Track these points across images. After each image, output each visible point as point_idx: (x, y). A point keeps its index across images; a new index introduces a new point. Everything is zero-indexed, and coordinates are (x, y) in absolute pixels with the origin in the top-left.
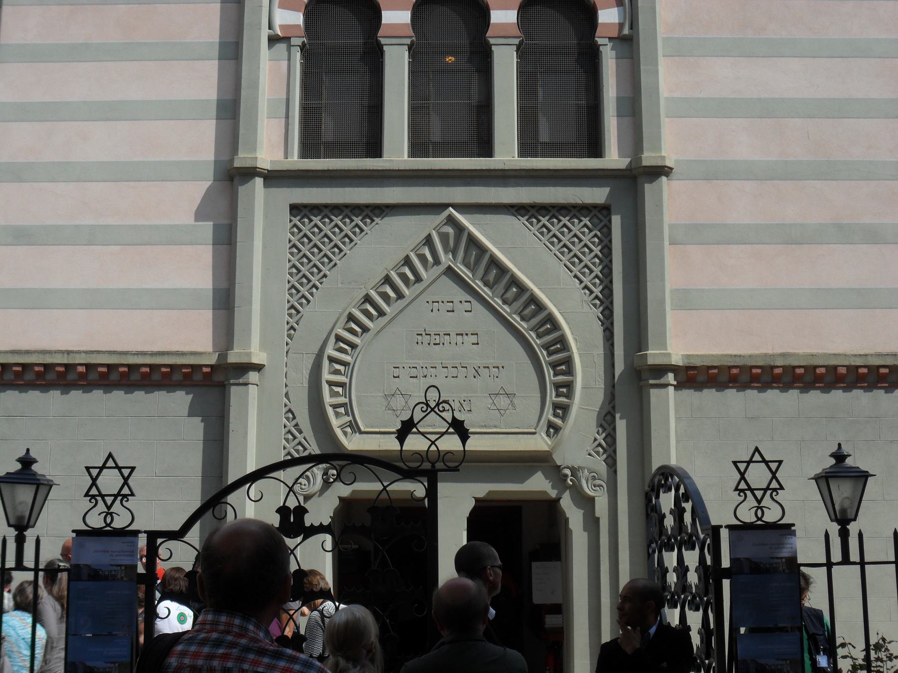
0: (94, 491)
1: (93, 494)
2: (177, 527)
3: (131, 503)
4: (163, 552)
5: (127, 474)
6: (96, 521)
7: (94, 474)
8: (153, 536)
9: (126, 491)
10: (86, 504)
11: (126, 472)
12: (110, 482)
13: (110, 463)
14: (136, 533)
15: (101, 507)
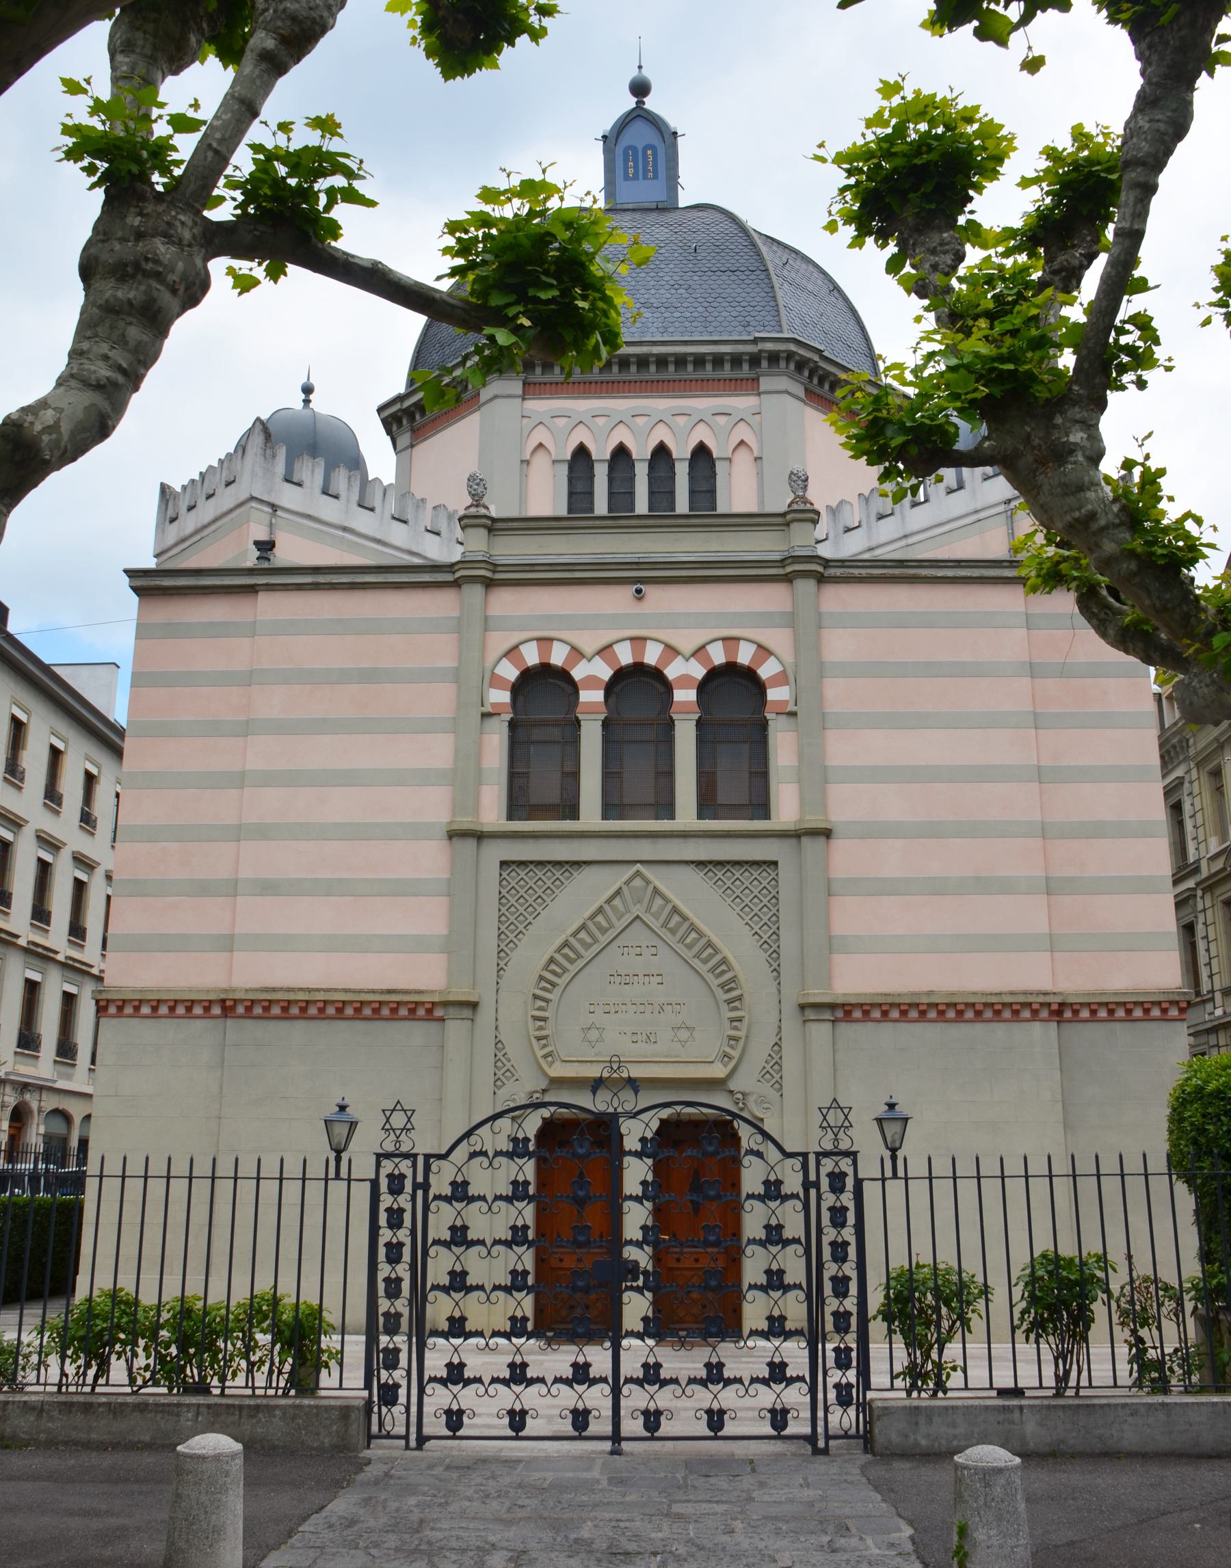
0: (387, 1126)
1: (387, 1129)
2: (443, 1152)
3: (412, 1134)
4: (434, 1168)
5: (410, 1114)
6: (389, 1147)
7: (388, 1114)
8: (427, 1157)
9: (409, 1126)
10: (383, 1134)
11: (409, 1113)
12: (398, 1120)
13: (399, 1107)
14: (415, 1156)
15: (392, 1137)
